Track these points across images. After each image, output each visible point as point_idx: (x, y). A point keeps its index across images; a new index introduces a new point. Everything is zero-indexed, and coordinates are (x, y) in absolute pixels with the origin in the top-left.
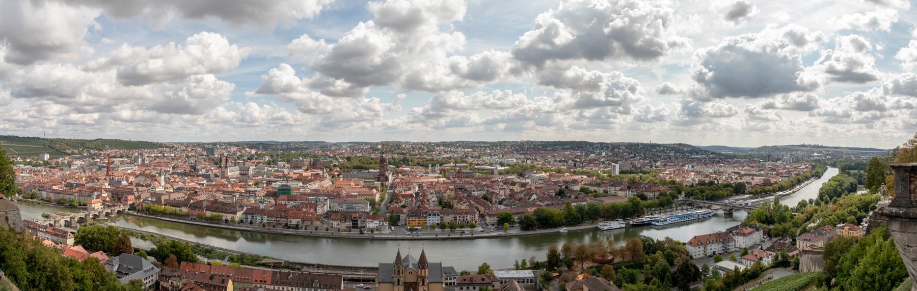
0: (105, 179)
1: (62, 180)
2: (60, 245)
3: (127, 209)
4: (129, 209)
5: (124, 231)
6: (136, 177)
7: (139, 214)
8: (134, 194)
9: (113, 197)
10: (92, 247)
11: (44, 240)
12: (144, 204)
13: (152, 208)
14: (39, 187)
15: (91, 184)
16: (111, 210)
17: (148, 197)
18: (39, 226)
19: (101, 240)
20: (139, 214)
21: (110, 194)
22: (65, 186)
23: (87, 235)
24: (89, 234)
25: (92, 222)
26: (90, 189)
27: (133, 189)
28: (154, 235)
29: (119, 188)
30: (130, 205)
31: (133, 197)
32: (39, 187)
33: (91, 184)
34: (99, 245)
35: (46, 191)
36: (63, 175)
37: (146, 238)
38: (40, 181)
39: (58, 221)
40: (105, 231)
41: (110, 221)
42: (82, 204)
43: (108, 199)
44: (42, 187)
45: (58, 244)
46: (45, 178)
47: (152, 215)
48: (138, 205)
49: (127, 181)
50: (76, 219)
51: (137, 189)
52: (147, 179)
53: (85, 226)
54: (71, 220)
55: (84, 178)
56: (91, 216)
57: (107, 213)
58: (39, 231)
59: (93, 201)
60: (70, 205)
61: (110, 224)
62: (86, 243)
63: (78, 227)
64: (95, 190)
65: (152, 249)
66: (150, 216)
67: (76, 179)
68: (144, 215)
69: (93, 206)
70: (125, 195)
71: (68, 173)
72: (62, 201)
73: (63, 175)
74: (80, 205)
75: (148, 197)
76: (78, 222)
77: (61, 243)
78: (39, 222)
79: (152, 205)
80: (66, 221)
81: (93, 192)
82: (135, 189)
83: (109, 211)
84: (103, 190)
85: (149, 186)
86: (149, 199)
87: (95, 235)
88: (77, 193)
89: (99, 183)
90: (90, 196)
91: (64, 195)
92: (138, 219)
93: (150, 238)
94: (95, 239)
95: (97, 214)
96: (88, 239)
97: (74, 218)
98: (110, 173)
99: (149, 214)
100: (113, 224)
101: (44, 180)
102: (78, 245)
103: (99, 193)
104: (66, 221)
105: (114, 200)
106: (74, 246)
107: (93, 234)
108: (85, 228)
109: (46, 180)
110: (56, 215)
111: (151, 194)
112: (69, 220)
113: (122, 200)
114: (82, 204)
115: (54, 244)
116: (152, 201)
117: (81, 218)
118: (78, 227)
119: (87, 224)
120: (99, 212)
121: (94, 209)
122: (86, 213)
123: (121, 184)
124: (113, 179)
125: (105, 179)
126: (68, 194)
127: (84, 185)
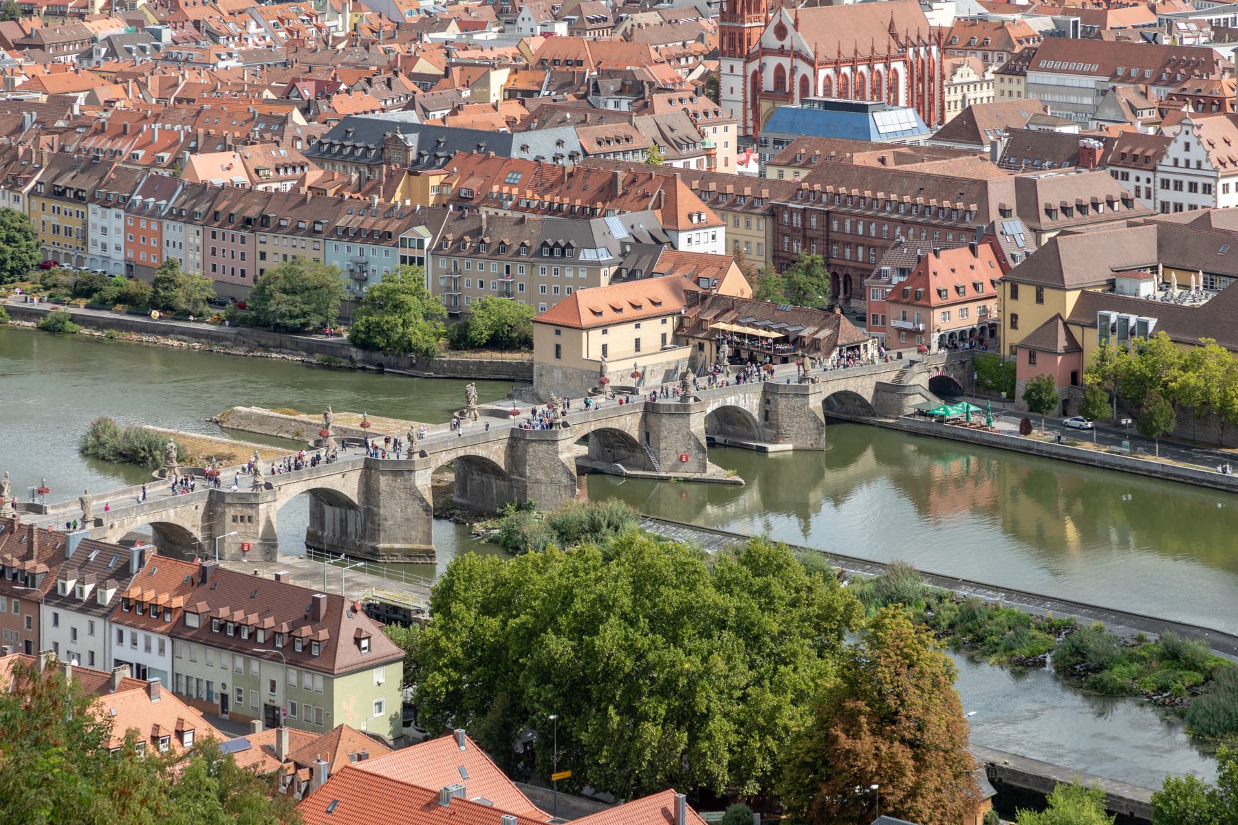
0: (711, 86)
1: (287, 95)
2: (262, 735)
3: (921, 379)
4: (942, 388)
5: (891, 598)
6: (1015, 68)
7: (1041, 436)
8: (990, 236)
9: (782, 261)
10: (578, 759)
11: (107, 686)
12: (1090, 340)
13: (1178, 379)
14: (62, 160)
15: (572, 138)
16: (770, 393)
17: (1135, 272)
18: (59, 556)
19: (666, 689)
20: (1041, 436)
21: (757, 233)
22: (320, 152)
23: (530, 636)
24: (546, 621)
25: (578, 504)
26: (564, 180)
27: (984, 185)
28: (1196, 647)
29: (846, 172)
30: (951, 341)
31: (984, 268)
32: (62, 160)
33: (572, 138)
34: (651, 732)
35: (124, 203)
36: (296, 43)
37: (1117, 675)
38: (62, 102)
39: (248, 502)
40: (710, 595)
41: (751, 496)
42: (482, 327)
43: (735, 285)
44: (92, 164)
45: (241, 726)
46: (119, 78)
47: (1174, 444)
48: (1033, 349)
49: (923, 103)
50: (423, 480)
51: (1026, 191)
52: (1126, 93)
53: (511, 545)
54: (368, 488)
55: (499, 79)
56: (570, 450)
57: (726, 418)
58: (54, 597)
59: (587, 298)
60: (363, 342)
61: (753, 528)
62: (518, 712)
63: (443, 563)
64: (608, 192)
65: (1176, 791)
66: (1156, 460)
67: (426, 81)
68: (1088, 447)
69: (592, 344)
70: (909, 247)
71: (340, 25)
72: (279, 304)
73: (296, 43)
74: (462, 341)
75: (1135, 272)
76: (445, 506)
77: (273, 719)
78: (54, 518)
79: (1169, 350)
80: (322, 499)
81: (588, 213)
82: (1002, 189)
83: (748, 401)
84: (686, 199)
85: (1147, 162)
86: (1148, 289)
87: (610, 635)
88: (431, 217)
89: (646, 127)
90: (558, 252)
91: (305, 249)
92: (1035, 487)
93: (1160, 673)
94: (608, 675)
95: (630, 424)
96: (544, 674)
97: (402, 471)
98: (755, 27)
99: (1145, 436)
100: (784, 529)
101: (106, 92)
102: (438, 731)
103: (649, 221)
104: (322, 499)
105: (798, 294)
106: (401, 741)
107: (587, 626)
108: (508, 567)
109: (125, 99)
110: (221, 442)
111: (1167, 239)
112: (349, 486)
113: (876, 293)
114: (482, 327)
115: (199, 726)
116: (1170, 316)
117: (471, 466)
118: (443, 563)
119: (534, 524)
120: (651, 409)
121: (596, 380)
122: (523, 412)
123: (862, 136)
124: (781, 91)
125: (711, 86)
126: (357, 235)
127: (498, 142)
